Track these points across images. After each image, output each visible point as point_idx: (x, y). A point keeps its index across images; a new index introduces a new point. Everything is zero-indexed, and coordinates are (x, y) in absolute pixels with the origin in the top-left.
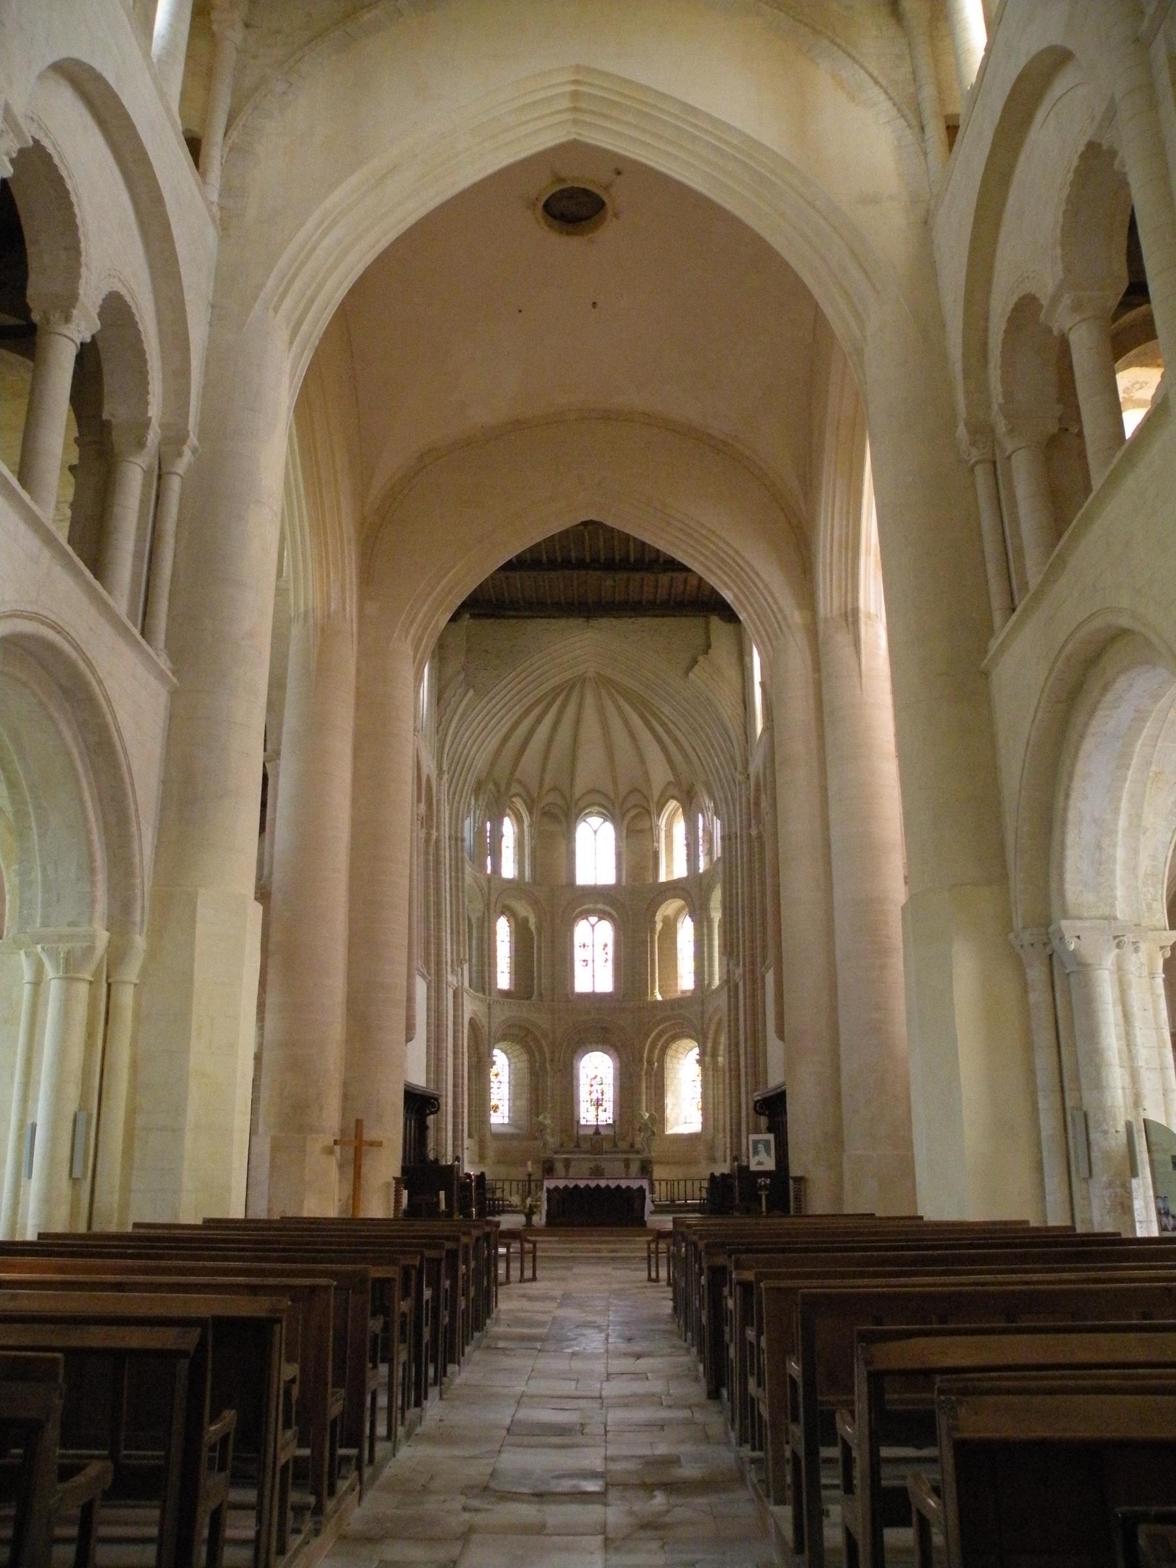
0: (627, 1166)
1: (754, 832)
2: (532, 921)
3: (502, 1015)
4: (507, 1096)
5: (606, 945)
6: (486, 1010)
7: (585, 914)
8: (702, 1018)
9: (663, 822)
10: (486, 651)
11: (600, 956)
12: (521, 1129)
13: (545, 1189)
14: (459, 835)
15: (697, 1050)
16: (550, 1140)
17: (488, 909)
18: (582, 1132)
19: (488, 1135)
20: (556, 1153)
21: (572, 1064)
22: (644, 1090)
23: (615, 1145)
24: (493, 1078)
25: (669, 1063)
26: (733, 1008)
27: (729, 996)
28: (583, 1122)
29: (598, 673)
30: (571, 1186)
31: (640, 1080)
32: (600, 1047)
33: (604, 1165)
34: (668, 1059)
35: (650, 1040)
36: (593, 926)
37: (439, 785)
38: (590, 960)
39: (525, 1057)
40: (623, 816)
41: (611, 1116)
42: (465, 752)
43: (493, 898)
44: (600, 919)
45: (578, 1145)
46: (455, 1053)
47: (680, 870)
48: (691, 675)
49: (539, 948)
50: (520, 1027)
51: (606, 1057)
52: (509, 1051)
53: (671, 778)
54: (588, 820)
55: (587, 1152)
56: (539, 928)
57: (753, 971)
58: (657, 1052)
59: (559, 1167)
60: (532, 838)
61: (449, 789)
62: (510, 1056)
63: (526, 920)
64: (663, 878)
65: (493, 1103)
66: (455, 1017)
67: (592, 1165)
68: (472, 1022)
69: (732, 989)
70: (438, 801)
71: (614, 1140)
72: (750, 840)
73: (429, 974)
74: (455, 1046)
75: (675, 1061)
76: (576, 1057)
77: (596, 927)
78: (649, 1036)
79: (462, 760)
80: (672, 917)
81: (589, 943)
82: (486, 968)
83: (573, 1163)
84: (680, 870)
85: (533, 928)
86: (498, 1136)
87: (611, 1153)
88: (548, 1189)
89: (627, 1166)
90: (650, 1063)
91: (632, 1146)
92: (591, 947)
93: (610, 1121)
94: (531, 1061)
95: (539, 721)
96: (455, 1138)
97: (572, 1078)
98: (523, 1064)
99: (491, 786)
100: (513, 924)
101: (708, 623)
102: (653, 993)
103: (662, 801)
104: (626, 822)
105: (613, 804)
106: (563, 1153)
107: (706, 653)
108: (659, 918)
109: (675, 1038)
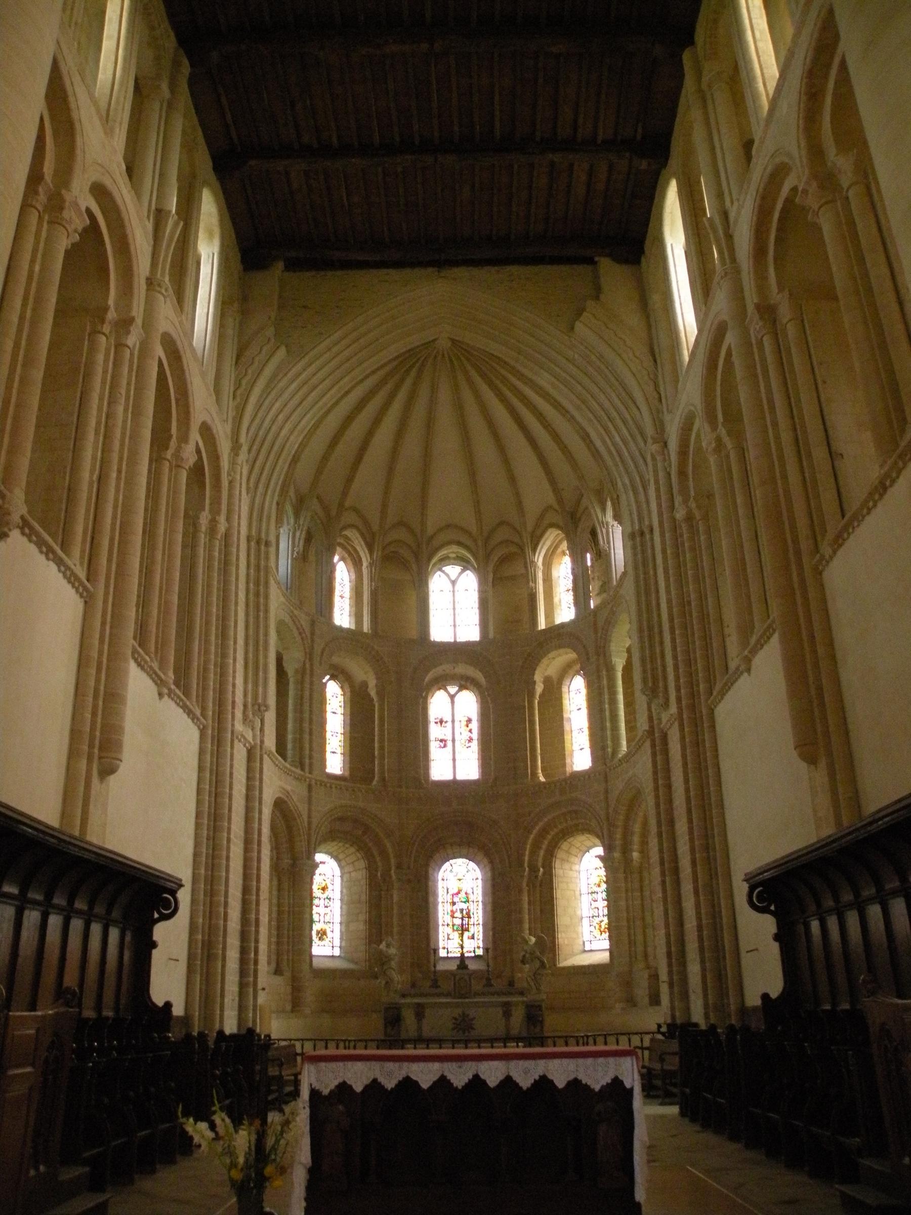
0: (507, 1014)
1: (680, 514)
2: (372, 683)
3: (325, 803)
4: (337, 919)
5: (469, 721)
6: (305, 793)
7: (441, 682)
8: (607, 798)
9: (539, 559)
10: (305, 307)
11: (462, 734)
12: (356, 963)
13: (305, 1094)
14: (263, 536)
15: (599, 850)
16: (396, 977)
17: (311, 659)
18: (441, 967)
19: (306, 967)
20: (404, 996)
21: (427, 872)
22: (526, 906)
23: (489, 984)
24: (316, 892)
25: (559, 869)
26: (662, 771)
27: (654, 755)
28: (442, 953)
29: (453, 341)
30: (390, 1084)
31: (520, 891)
32: (464, 851)
33: (472, 1013)
34: (557, 864)
35: (532, 836)
36: (452, 697)
37: (233, 463)
38: (449, 737)
39: (362, 864)
40: (488, 556)
41: (481, 945)
42: (274, 428)
43: (318, 649)
44: (462, 688)
45: (435, 984)
46: (247, 842)
47: (566, 613)
48: (578, 326)
49: (382, 719)
50: (356, 821)
51: (472, 865)
52: (341, 856)
53: (551, 499)
54: (445, 569)
55: (448, 995)
56: (381, 694)
57: (693, 708)
58: (542, 853)
59: (409, 1017)
60: (371, 580)
61: (250, 473)
62: (343, 863)
63: (365, 685)
64: (542, 625)
65: (316, 927)
66: (249, 788)
67: (457, 1012)
68: (279, 805)
69: (658, 742)
70: (230, 482)
71: (487, 978)
72: (675, 528)
73: (204, 715)
74: (248, 830)
75: (566, 866)
76: (432, 864)
77: (456, 699)
78: (530, 832)
79: (270, 437)
80: (555, 680)
81: (447, 717)
82: (307, 736)
83: (428, 1012)
84: (566, 613)
85: (373, 693)
86: (323, 973)
87: (484, 994)
88: (315, 1094)
89: (507, 1014)
90: (534, 869)
91: (511, 984)
92: (449, 725)
93: (480, 952)
94: (371, 870)
95: (377, 421)
96: (243, 972)
97: (427, 893)
98: (361, 875)
99: (315, 505)
100: (348, 690)
101: (596, 277)
102: (534, 774)
103: (538, 533)
104: (490, 568)
105: (475, 541)
106: (415, 996)
107: (597, 298)
108: (538, 677)
109: (566, 834)
